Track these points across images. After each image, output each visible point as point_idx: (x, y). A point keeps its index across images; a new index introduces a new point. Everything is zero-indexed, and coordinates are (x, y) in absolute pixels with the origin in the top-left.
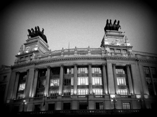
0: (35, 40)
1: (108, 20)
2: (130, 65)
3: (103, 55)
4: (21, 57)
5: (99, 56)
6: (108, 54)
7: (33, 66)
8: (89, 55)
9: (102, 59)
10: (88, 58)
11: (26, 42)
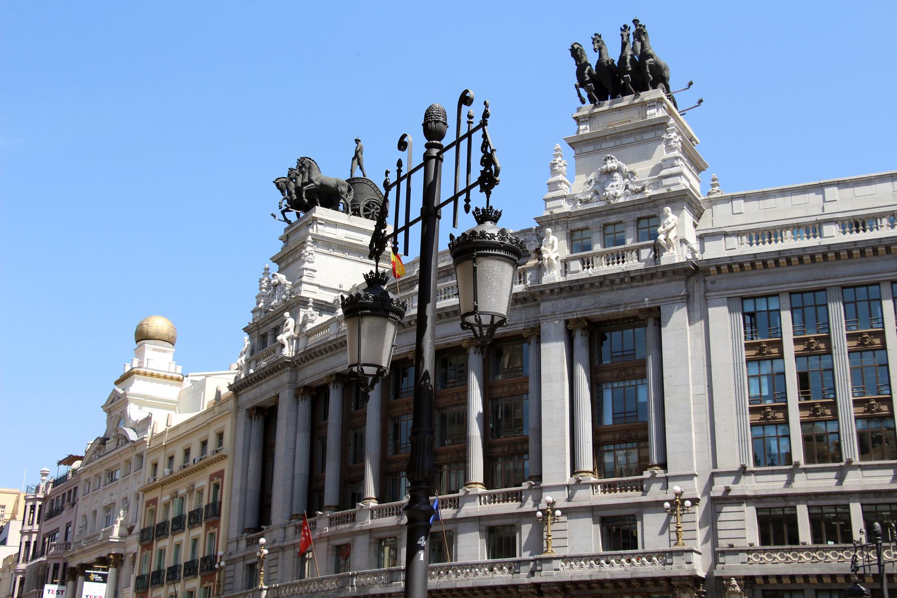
1: (576, 53)
2: (659, 308)
4: (262, 331)
7: (285, 377)
11: (277, 247)
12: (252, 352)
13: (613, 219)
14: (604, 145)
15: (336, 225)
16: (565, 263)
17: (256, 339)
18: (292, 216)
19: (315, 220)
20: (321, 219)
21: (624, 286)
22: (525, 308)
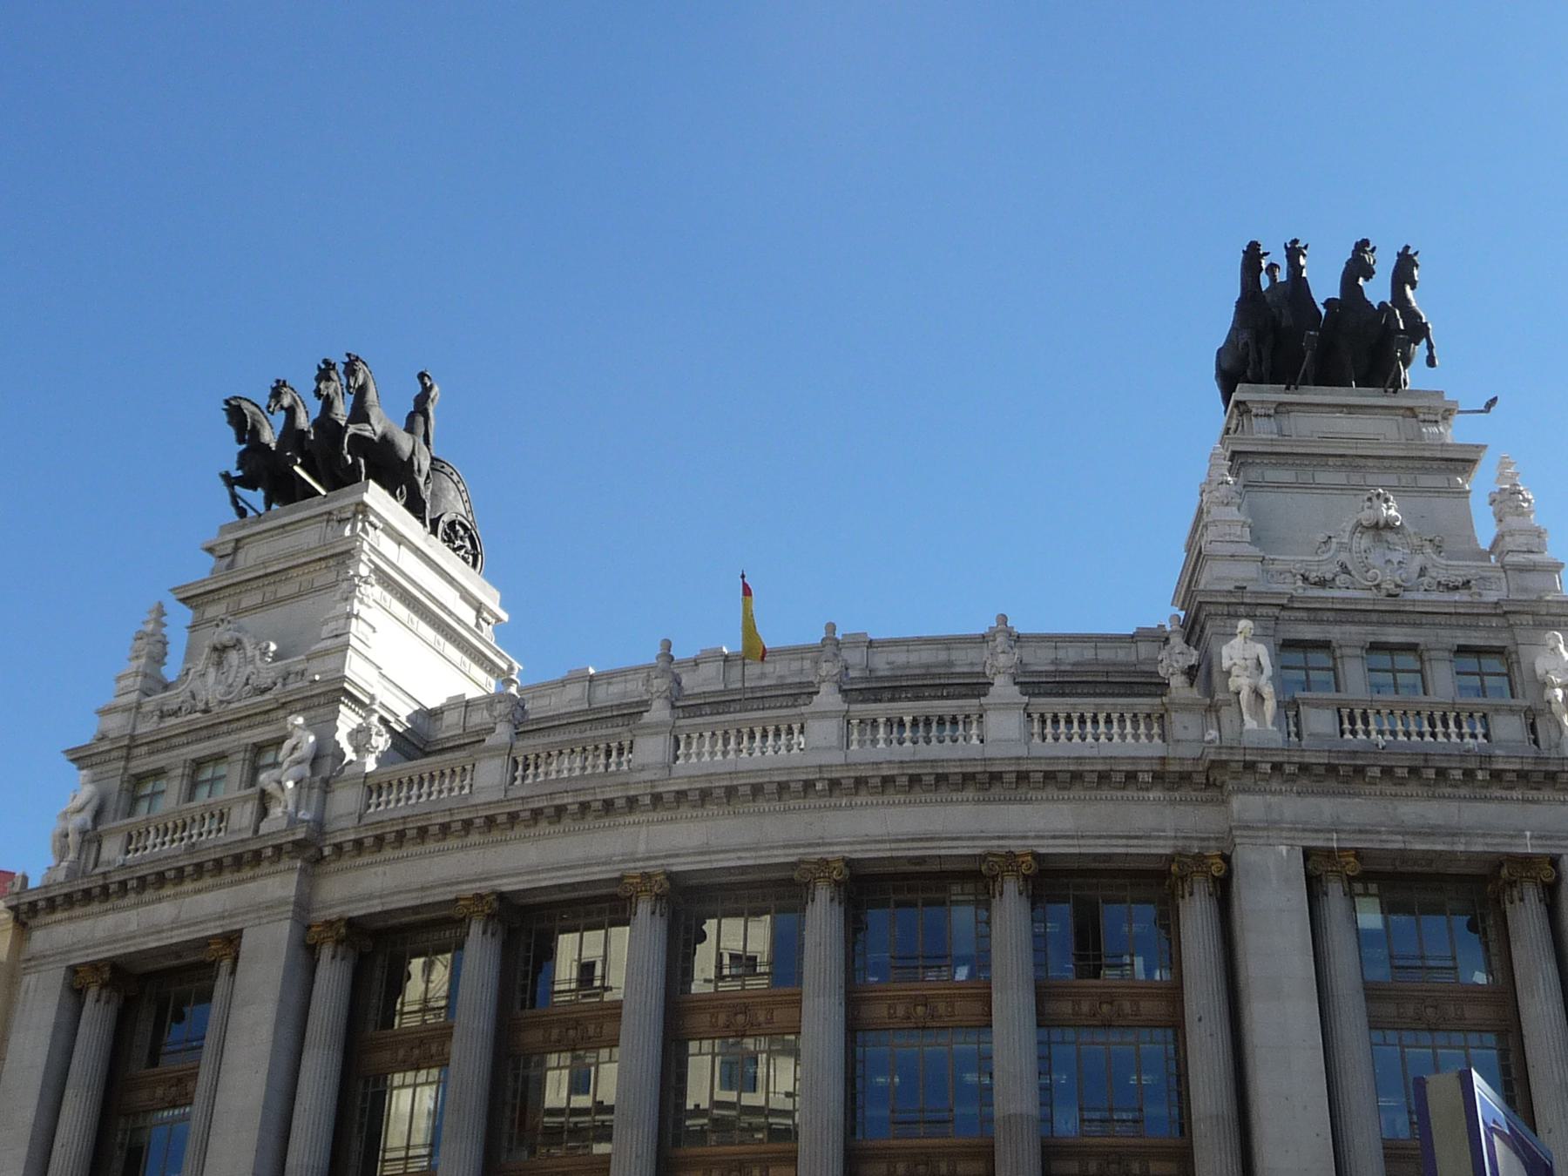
0: (310, 537)
2: (1554, 861)
3: (1191, 736)
4: (141, 765)
5: (1130, 744)
6: (1250, 723)
7: (280, 885)
8: (1003, 731)
9: (1168, 778)
10: (985, 781)
12: (98, 815)
13: (1395, 635)
14: (1323, 477)
15: (400, 539)
16: (1290, 709)
17: (115, 784)
18: (255, 498)
19: (363, 509)
20: (378, 516)
21: (1463, 791)
22: (1172, 802)
